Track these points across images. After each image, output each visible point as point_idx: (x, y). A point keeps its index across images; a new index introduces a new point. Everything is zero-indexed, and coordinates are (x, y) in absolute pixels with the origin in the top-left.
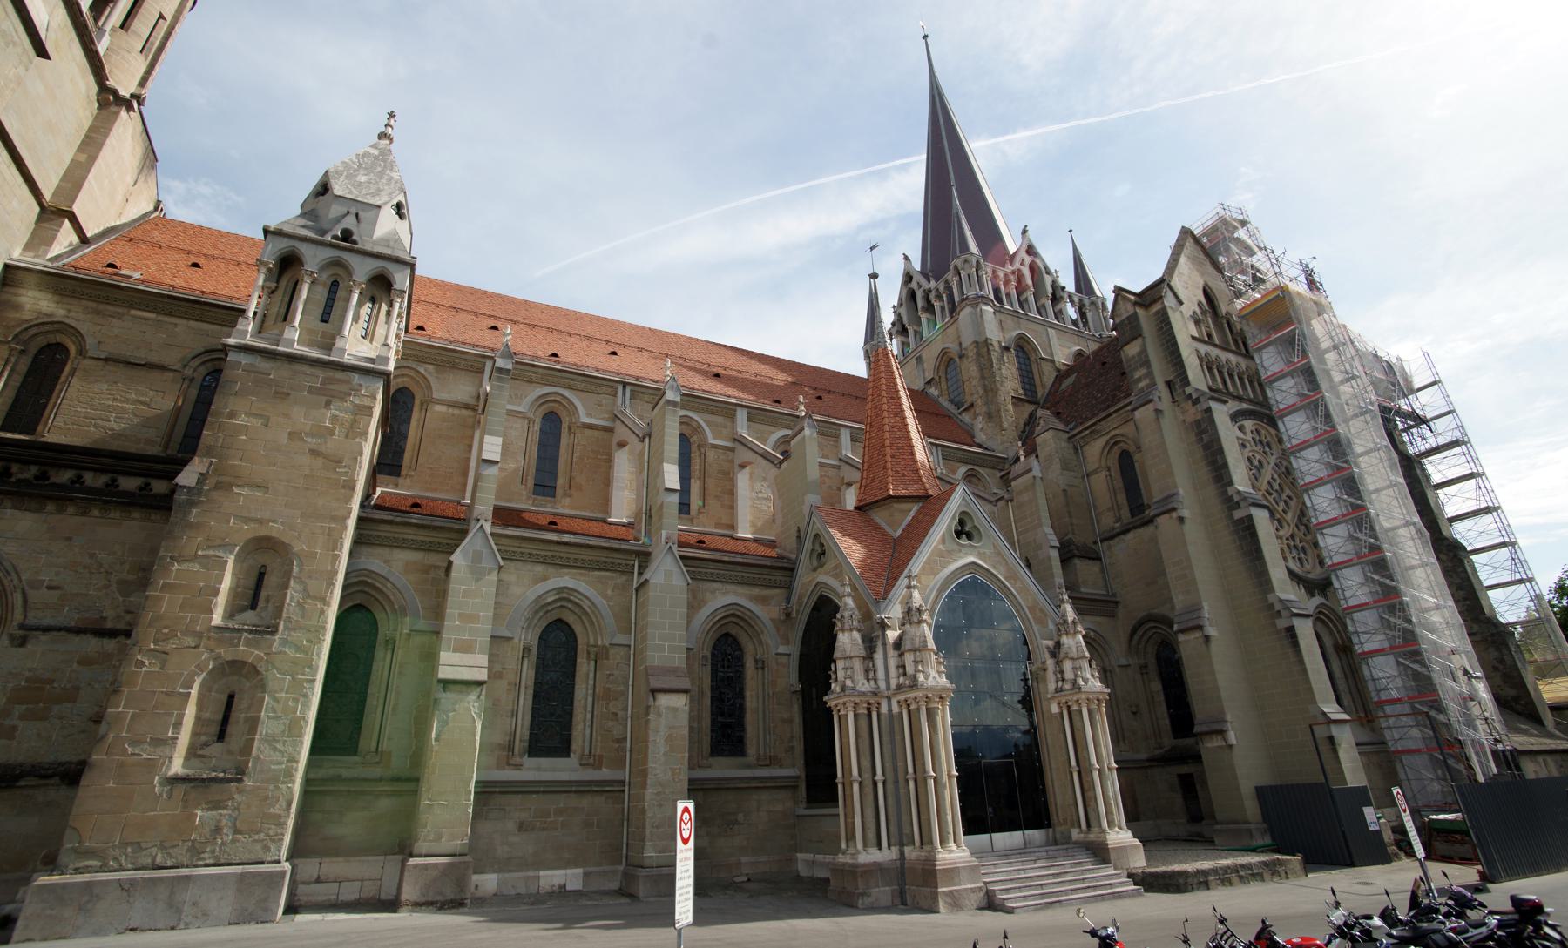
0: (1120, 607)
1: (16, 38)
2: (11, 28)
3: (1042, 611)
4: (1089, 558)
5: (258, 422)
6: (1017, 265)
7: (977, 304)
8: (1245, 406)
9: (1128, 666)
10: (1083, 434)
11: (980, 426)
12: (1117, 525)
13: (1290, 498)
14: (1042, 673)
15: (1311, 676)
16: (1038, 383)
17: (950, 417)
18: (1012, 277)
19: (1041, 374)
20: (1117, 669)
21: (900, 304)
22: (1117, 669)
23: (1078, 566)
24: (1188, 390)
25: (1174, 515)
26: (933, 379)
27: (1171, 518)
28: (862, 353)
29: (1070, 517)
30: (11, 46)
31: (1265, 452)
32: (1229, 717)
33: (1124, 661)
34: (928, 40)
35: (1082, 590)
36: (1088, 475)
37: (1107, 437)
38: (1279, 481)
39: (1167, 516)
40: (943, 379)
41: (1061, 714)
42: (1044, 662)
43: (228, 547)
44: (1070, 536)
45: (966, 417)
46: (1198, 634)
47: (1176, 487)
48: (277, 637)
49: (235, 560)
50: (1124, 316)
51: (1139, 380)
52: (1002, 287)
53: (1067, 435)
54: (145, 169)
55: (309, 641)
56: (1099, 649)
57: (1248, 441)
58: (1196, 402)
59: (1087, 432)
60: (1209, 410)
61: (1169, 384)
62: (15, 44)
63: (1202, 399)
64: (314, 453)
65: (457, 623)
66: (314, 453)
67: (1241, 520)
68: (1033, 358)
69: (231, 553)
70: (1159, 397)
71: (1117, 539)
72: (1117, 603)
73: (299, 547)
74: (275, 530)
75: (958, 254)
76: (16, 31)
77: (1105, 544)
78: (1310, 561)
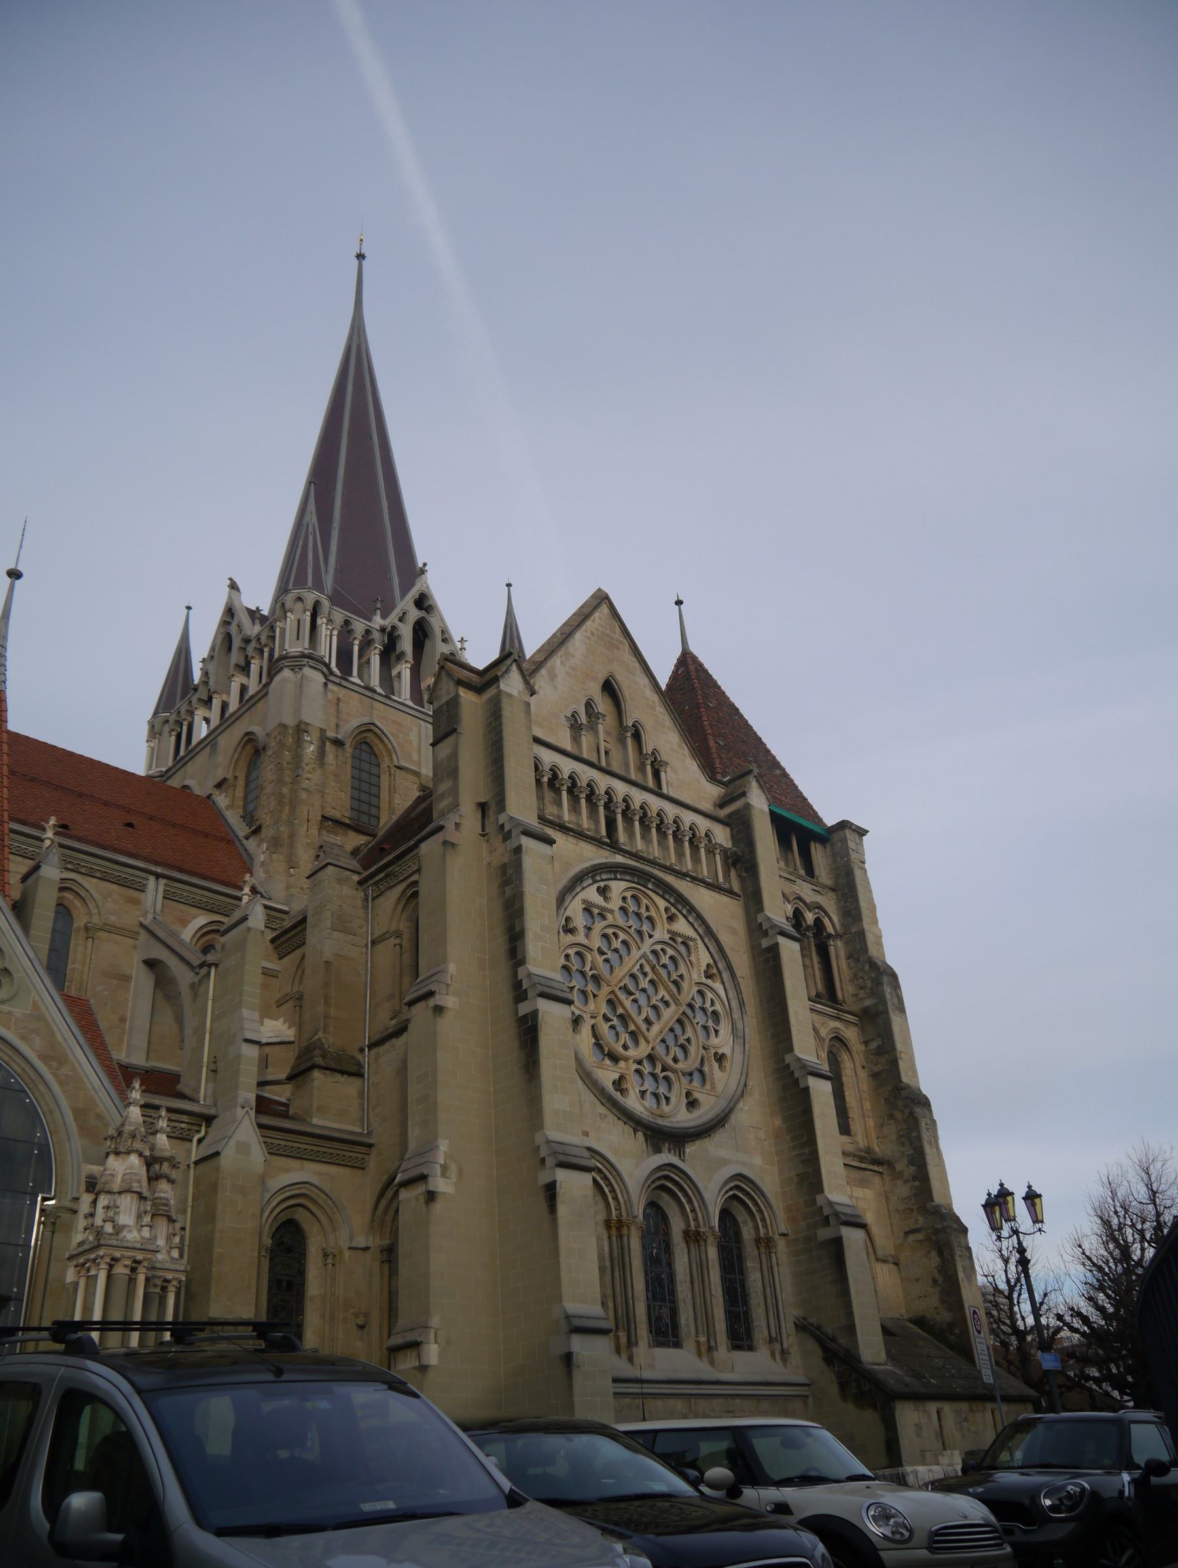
0: (374, 1151)
3: (99, 1117)
4: (343, 1072)
6: (392, 619)
7: (301, 667)
8: (619, 859)
9: (366, 1249)
10: (377, 878)
11: (262, 858)
12: (393, 1022)
13: (667, 1004)
14: (65, 1216)
15: (563, 1259)
16: (384, 804)
17: (230, 842)
18: (376, 635)
19: (392, 790)
20: (347, 1254)
21: (211, 657)
22: (347, 1254)
23: (316, 1083)
24: (502, 819)
25: (432, 1002)
26: (225, 780)
27: (427, 1006)
28: (145, 728)
29: (326, 1002)
31: (640, 933)
32: (435, 1322)
33: (361, 1242)
34: (364, 263)
35: (315, 1121)
36: (373, 943)
37: (403, 886)
38: (651, 976)
39: (421, 1005)
40: (241, 782)
41: (76, 1284)
42: (76, 1199)
44: (320, 1035)
45: (251, 845)
46: (420, 1189)
47: (445, 961)
50: (444, 700)
51: (442, 796)
52: (356, 649)
53: (356, 878)
56: (323, 1218)
57: (612, 912)
58: (507, 836)
59: (382, 875)
60: (518, 850)
61: (483, 807)
63: (514, 833)
67: (525, 1017)
68: (385, 763)
70: (457, 825)
71: (387, 1046)
72: (370, 1146)
75: (290, 587)
77: (374, 1051)
78: (673, 1100)
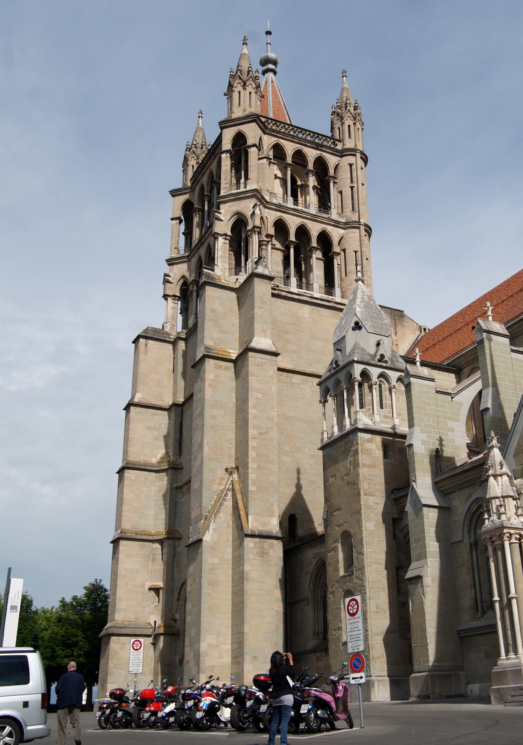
1: (264, 361)
2: (260, 359)
5: (333, 479)
30: (264, 365)
43: (337, 541)
48: (354, 576)
49: (342, 545)
54: (397, 322)
55: (362, 575)
62: (265, 363)
64: (348, 483)
65: (414, 545)
66: (348, 483)
69: (339, 542)
73: (352, 531)
74: (346, 527)
76: (262, 359)
